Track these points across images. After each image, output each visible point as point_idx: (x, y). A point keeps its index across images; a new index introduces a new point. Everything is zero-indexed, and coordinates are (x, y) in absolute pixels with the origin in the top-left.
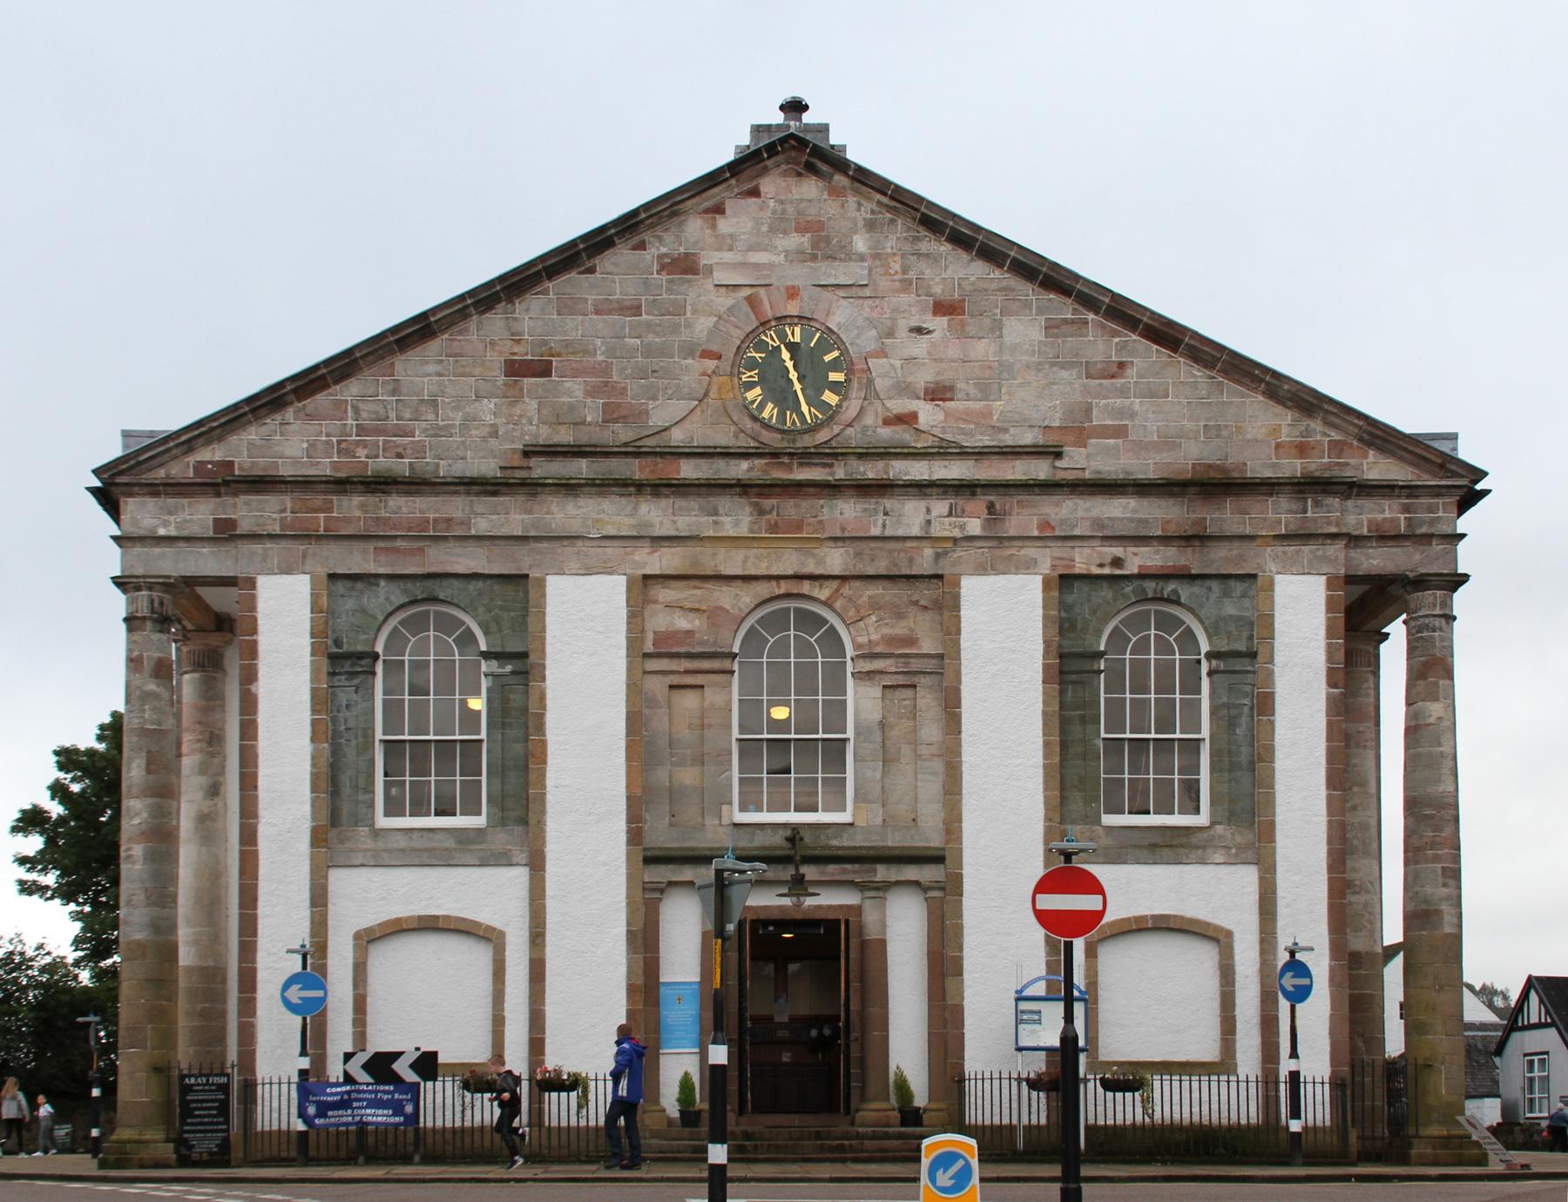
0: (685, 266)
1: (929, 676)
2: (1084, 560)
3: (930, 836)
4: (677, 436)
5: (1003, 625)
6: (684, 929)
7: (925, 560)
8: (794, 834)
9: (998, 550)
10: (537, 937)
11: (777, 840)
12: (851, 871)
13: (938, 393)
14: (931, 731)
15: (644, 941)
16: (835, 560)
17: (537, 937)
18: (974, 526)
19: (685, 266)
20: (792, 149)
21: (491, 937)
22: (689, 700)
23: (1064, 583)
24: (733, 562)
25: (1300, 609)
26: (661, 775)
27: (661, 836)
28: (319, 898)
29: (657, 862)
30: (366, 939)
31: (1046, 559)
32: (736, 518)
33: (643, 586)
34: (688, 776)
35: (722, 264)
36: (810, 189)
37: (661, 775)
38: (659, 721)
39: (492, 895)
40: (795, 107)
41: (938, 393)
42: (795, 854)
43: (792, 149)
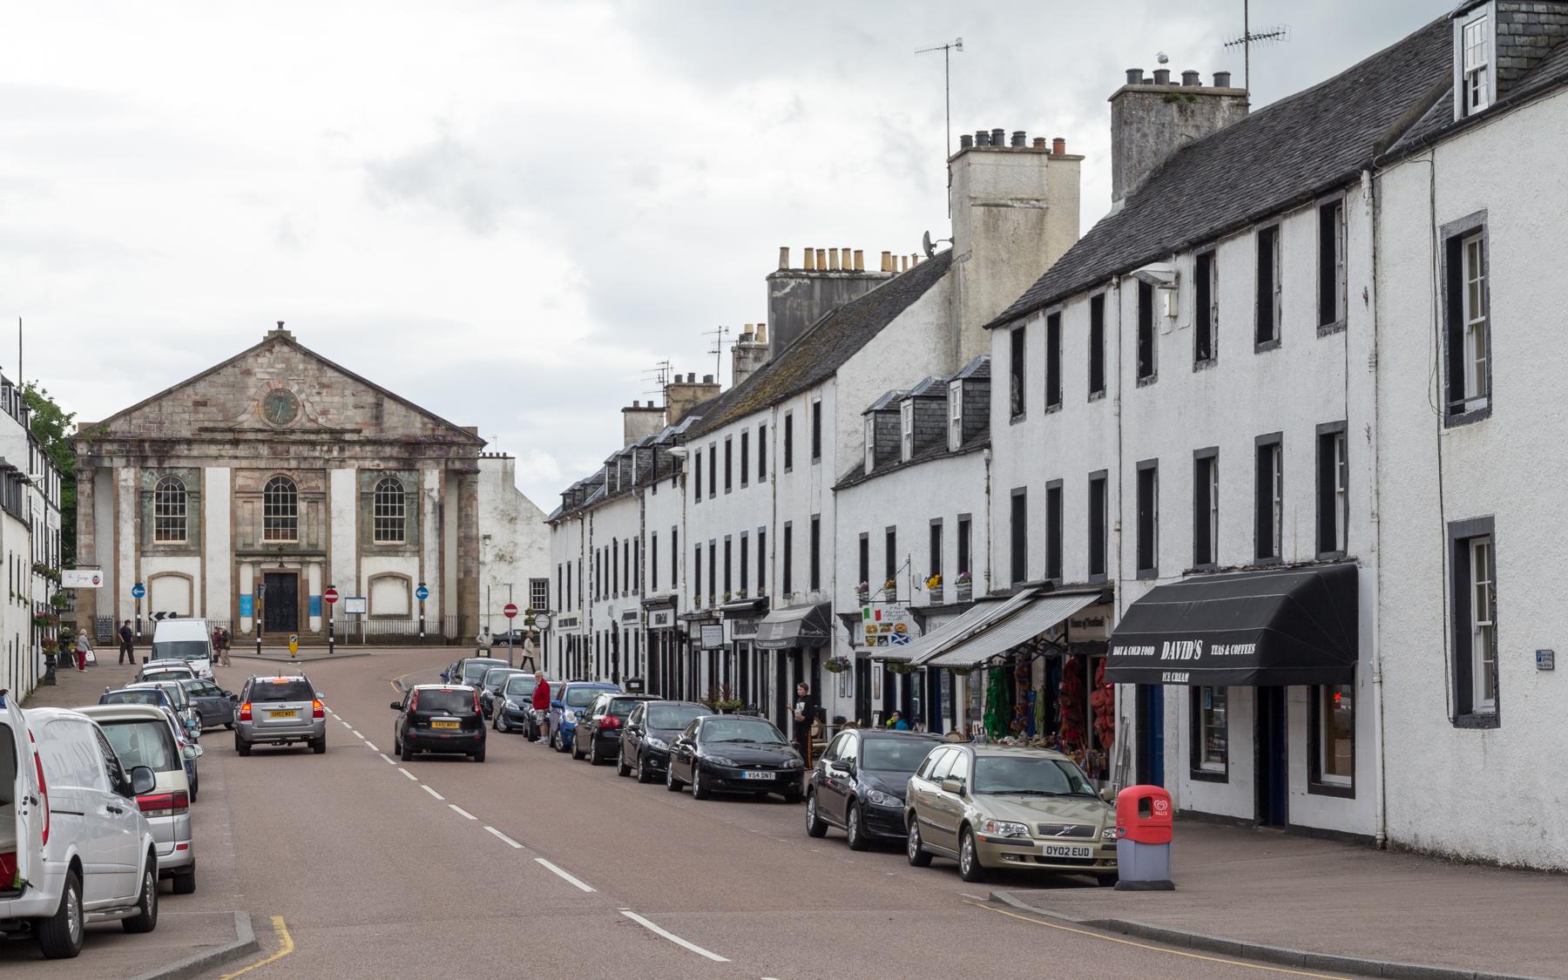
0: (248, 373)
1: (321, 498)
2: (368, 464)
3: (322, 547)
4: (246, 426)
5: (344, 485)
6: (248, 575)
7: (319, 464)
8: (281, 547)
9: (342, 463)
10: (203, 578)
11: (275, 549)
12: (298, 559)
13: (324, 413)
14: (322, 516)
15: (236, 580)
16: (293, 464)
17: (203, 578)
18: (335, 453)
19: (248, 373)
20: (280, 338)
21: (189, 578)
22: (249, 506)
23: (361, 471)
24: (262, 464)
25: (432, 479)
26: (241, 529)
27: (240, 547)
28: (138, 567)
29: (241, 554)
30: (152, 578)
31: (356, 464)
32: (264, 450)
33: (236, 471)
34: (249, 529)
35: (260, 373)
36: (286, 349)
37: (241, 529)
38: (239, 513)
39: (189, 565)
40: (281, 324)
41: (324, 413)
42: (280, 553)
43: (280, 338)
